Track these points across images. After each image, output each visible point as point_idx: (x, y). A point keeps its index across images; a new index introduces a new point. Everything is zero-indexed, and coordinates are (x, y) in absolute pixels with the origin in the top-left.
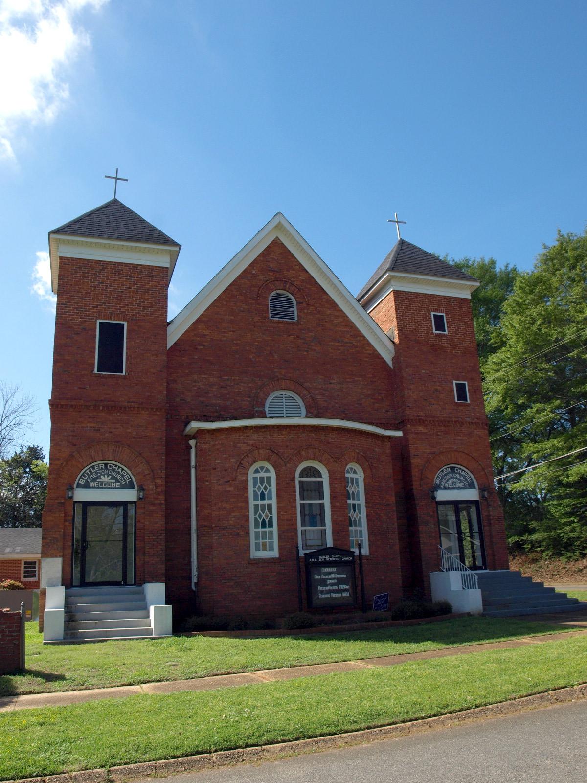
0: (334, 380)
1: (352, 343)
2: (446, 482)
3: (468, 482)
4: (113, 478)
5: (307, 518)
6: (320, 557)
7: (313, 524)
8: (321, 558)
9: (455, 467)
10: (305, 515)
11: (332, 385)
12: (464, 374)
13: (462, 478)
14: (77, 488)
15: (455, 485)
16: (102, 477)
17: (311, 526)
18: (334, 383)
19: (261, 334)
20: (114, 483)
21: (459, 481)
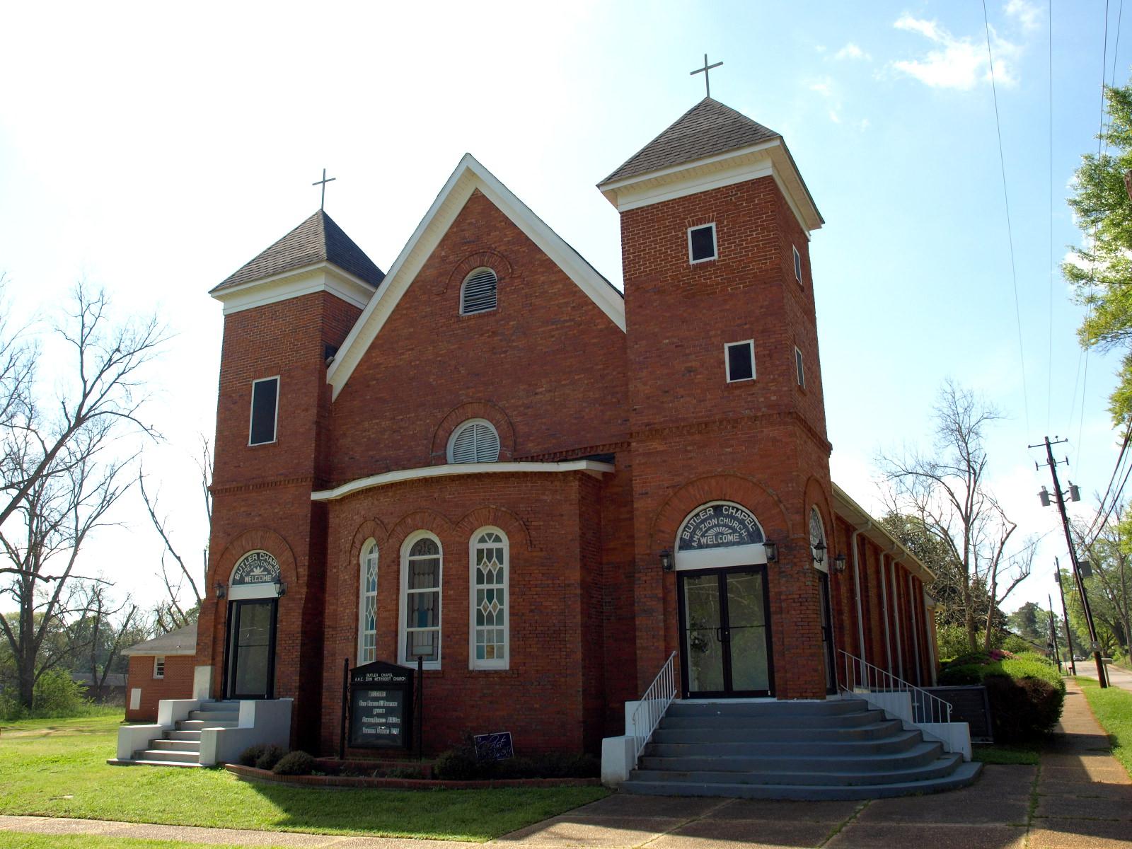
0: (543, 387)
1: (573, 320)
2: (703, 536)
3: (748, 530)
4: (266, 570)
5: (416, 614)
6: (368, 675)
7: (423, 623)
8: (369, 678)
9: (723, 506)
11: (538, 397)
12: (747, 326)
13: (736, 524)
15: (721, 539)
16: (255, 569)
17: (419, 626)
18: (541, 393)
19: (445, 343)
20: (265, 575)
21: (731, 531)
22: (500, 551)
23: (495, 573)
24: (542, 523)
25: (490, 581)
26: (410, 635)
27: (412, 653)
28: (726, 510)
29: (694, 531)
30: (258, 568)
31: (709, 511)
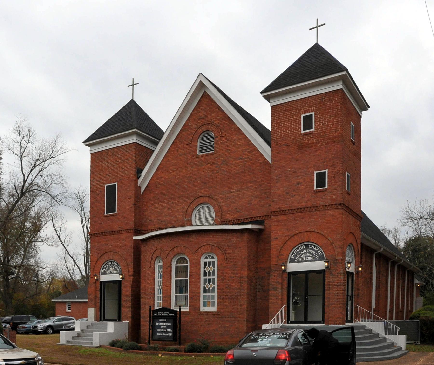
0: (234, 189)
2: (300, 257)
3: (319, 255)
4: (115, 268)
6: (159, 313)
7: (181, 292)
8: (159, 314)
9: (309, 244)
10: (177, 287)
11: (232, 194)
13: (314, 252)
14: (102, 274)
15: (307, 258)
16: (110, 268)
17: (180, 293)
18: (233, 192)
20: (115, 271)
21: (311, 255)
22: (213, 263)
23: (211, 272)
24: (231, 251)
25: (209, 275)
26: (176, 297)
27: (177, 304)
28: (310, 246)
29: (296, 255)
30: (112, 268)
31: (303, 246)
